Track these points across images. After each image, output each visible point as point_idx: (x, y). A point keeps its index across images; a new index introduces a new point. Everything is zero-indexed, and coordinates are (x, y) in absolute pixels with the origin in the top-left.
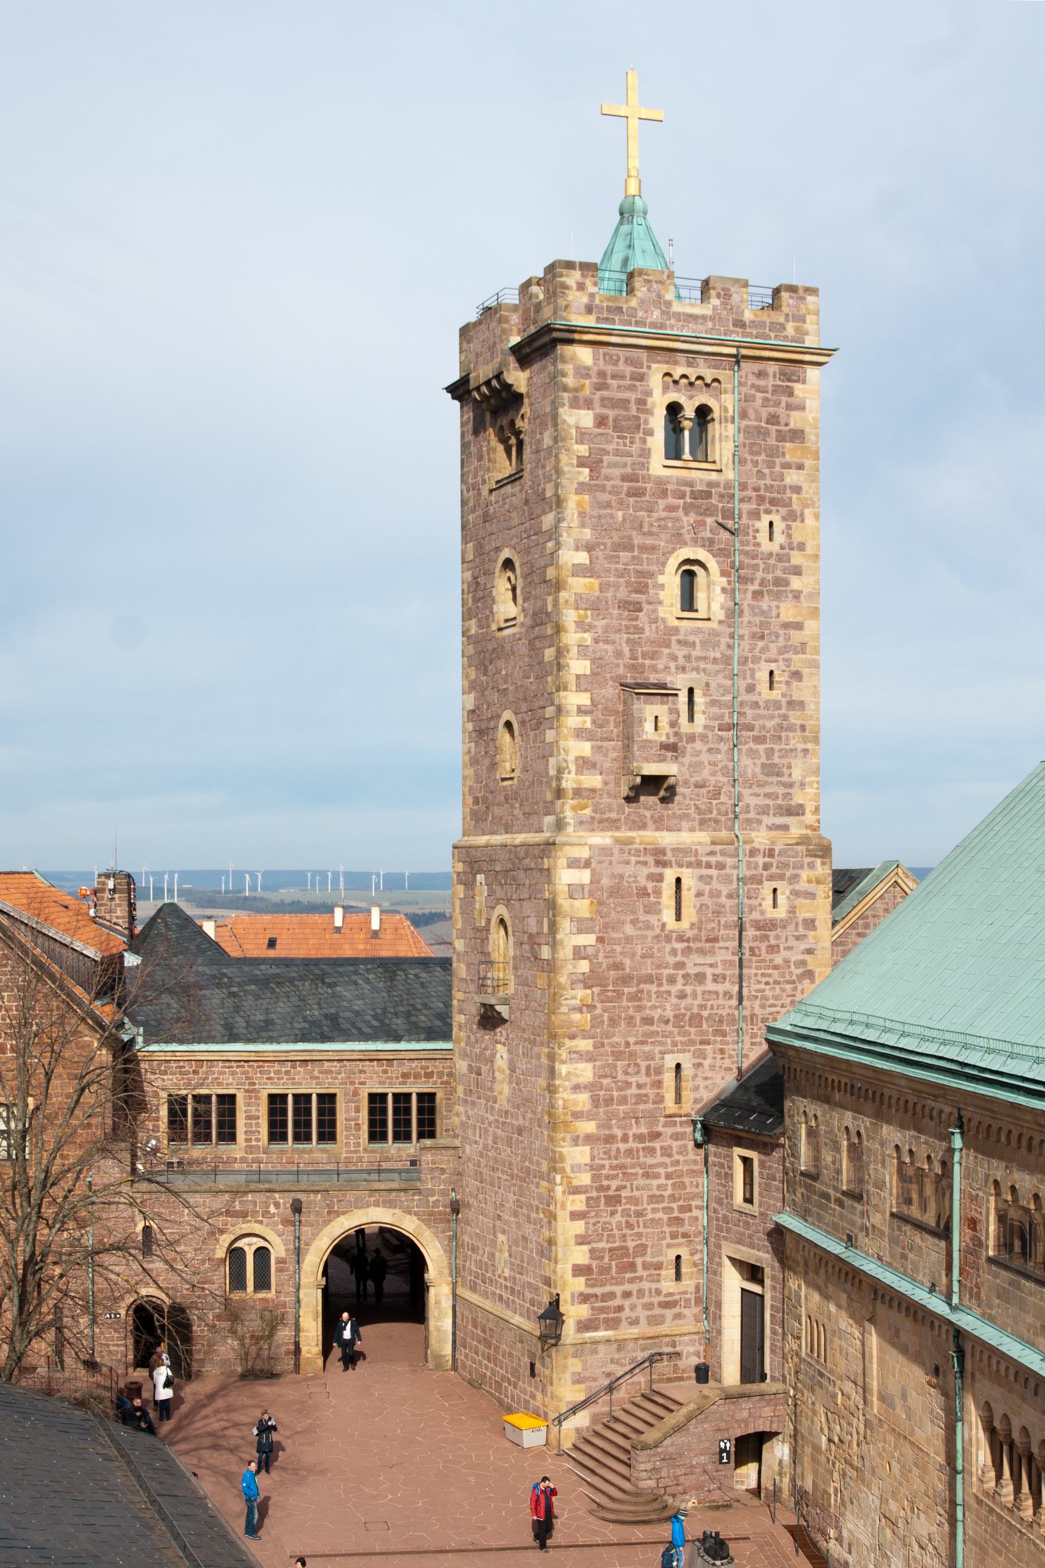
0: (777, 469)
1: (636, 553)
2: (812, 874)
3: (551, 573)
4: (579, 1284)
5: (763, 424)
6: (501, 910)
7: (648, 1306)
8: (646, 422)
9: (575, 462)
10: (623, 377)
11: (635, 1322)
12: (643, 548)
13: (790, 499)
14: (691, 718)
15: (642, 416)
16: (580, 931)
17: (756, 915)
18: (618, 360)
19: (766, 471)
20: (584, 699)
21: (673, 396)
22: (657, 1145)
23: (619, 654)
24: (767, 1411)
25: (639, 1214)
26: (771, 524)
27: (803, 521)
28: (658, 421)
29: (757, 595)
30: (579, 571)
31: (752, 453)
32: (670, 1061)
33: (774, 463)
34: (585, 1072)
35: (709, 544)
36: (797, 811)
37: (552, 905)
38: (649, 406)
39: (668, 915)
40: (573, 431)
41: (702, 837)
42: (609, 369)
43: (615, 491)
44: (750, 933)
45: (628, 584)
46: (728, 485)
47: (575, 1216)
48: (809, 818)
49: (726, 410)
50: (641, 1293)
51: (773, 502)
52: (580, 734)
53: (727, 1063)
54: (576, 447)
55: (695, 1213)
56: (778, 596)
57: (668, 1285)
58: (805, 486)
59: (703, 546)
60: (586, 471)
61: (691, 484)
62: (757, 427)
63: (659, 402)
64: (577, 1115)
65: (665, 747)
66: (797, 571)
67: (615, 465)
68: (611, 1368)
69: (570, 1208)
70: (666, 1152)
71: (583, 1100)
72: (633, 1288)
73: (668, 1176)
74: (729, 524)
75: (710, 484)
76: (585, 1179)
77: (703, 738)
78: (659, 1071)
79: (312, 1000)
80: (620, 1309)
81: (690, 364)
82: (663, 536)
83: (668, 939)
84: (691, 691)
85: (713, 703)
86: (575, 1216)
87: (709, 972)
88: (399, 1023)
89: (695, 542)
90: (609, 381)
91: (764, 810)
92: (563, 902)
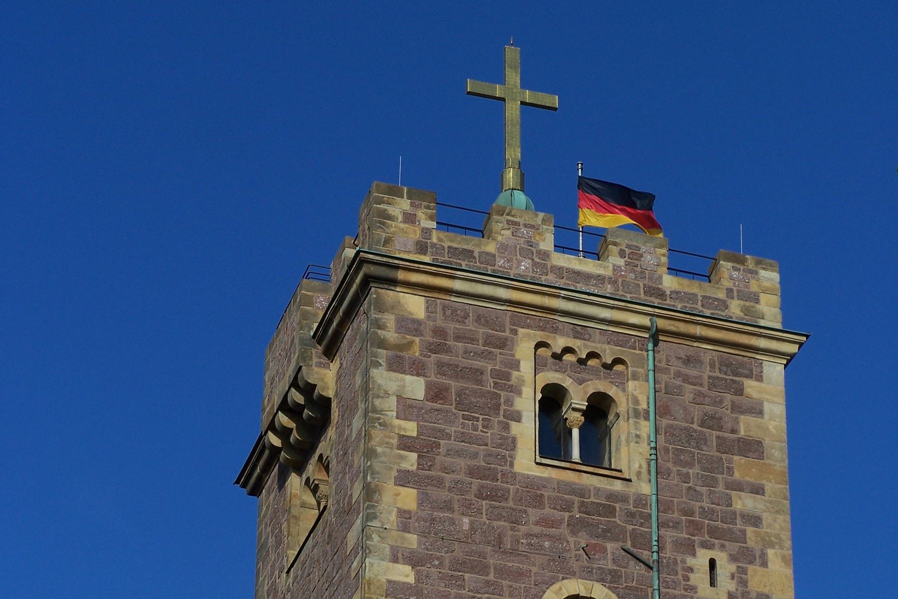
0: (721, 488)
1: (491, 577)
5: (695, 426)
8: (509, 402)
9: (395, 441)
10: (473, 340)
12: (501, 572)
13: (744, 532)
15: (503, 394)
18: (466, 316)
19: (704, 490)
21: (551, 377)
26: (712, 563)
27: (764, 564)
28: (527, 404)
31: (678, 462)
33: (715, 480)
38: (514, 380)
40: (392, 402)
42: (452, 327)
43: (458, 487)
46: (641, 501)
49: (636, 401)
51: (713, 532)
54: (397, 422)
58: (767, 518)
59: (601, 580)
60: (414, 456)
61: (582, 492)
62: (685, 429)
67: (459, 453)
74: (645, 554)
75: (613, 496)
81: (577, 336)
82: (539, 559)
89: (588, 574)
90: (451, 343)
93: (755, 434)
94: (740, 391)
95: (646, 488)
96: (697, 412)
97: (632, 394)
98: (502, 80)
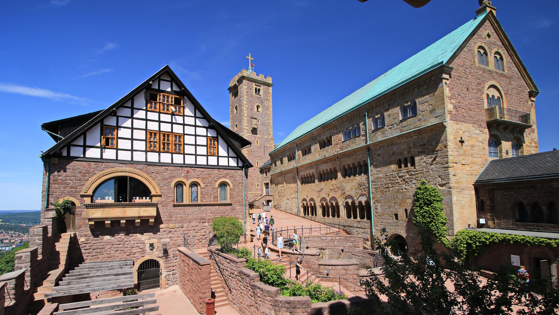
63: (255, 87)
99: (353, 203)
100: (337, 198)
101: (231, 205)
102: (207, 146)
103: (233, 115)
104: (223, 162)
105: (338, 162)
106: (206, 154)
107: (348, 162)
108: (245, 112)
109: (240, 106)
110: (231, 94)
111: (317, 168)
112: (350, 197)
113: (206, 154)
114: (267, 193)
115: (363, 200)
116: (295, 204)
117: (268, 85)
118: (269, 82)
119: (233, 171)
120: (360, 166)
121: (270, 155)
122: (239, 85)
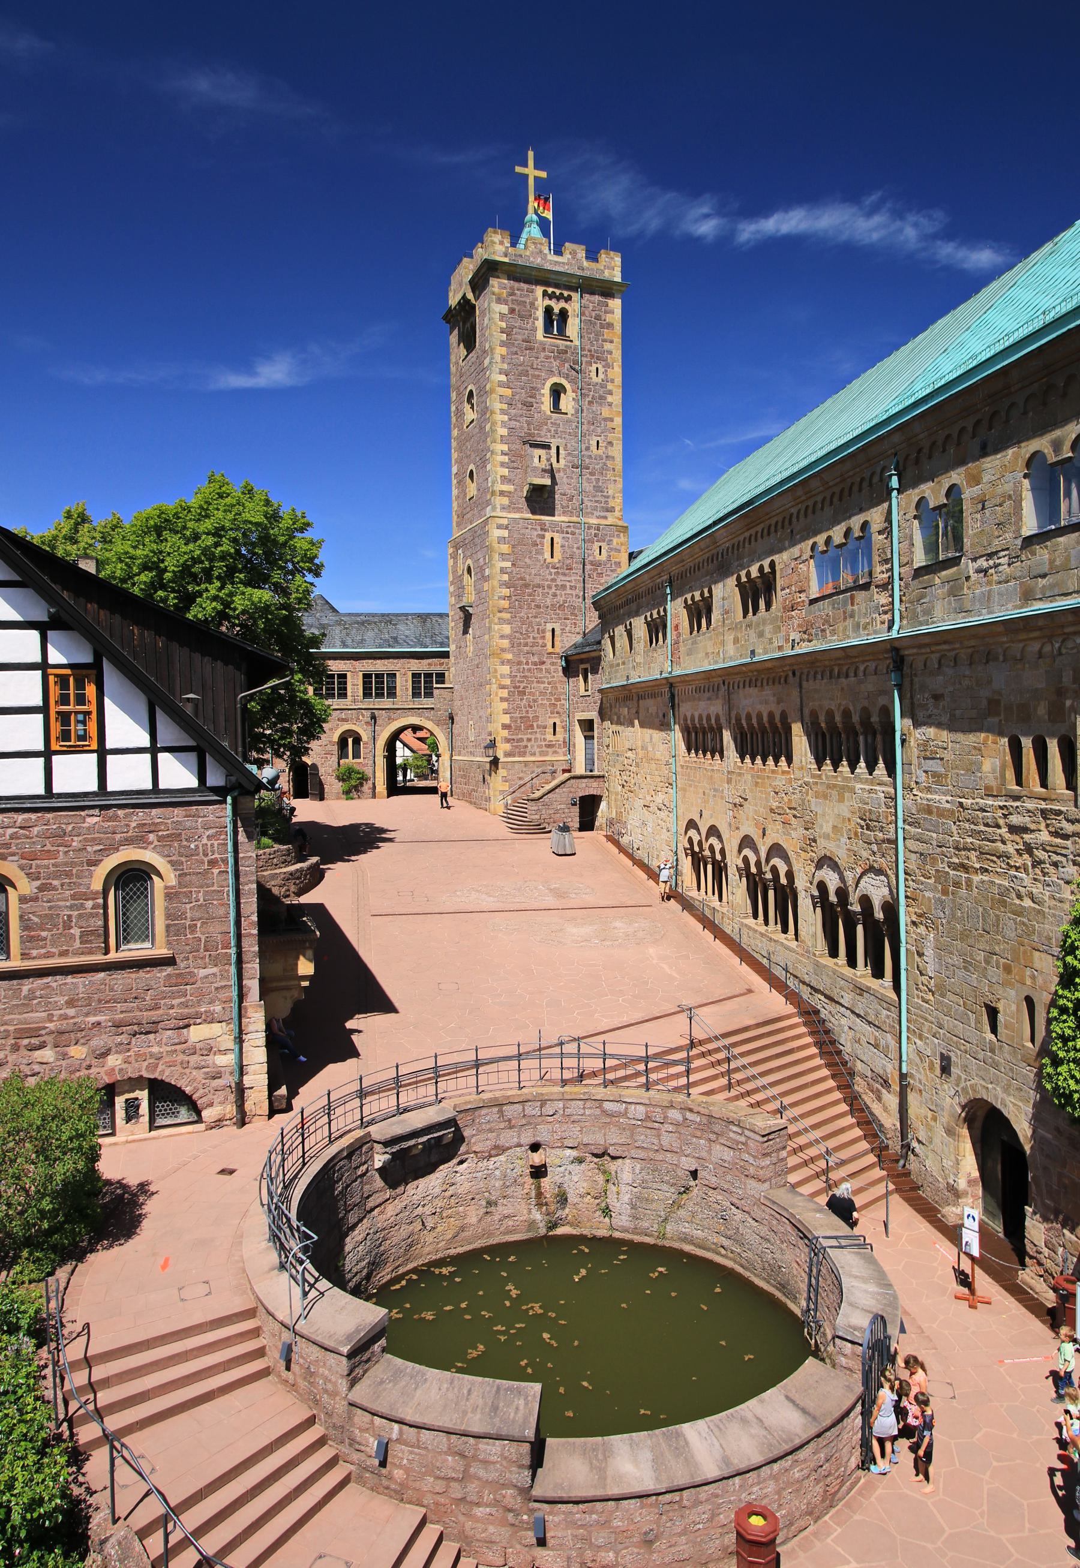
2: (619, 540)
3: (488, 388)
4: (505, 733)
6: (469, 562)
7: (540, 746)
11: (534, 754)
12: (534, 376)
14: (558, 461)
16: (503, 560)
17: (591, 558)
20: (505, 448)
22: (543, 667)
23: (521, 427)
24: (595, 784)
25: (535, 701)
28: (540, 314)
29: (590, 403)
30: (501, 384)
32: (549, 627)
34: (507, 629)
35: (567, 377)
36: (611, 510)
37: (489, 549)
39: (547, 555)
41: (566, 519)
42: (516, 285)
44: (588, 567)
45: (526, 393)
46: (576, 347)
47: (502, 699)
48: (617, 514)
50: (536, 739)
51: (598, 358)
52: (502, 464)
53: (578, 630)
55: (563, 702)
56: (601, 405)
57: (550, 737)
63: (541, 303)
64: (503, 650)
65: (544, 470)
66: (610, 393)
68: (521, 775)
69: (500, 695)
70: (548, 671)
71: (505, 643)
72: (533, 737)
73: (549, 683)
75: (566, 346)
76: (508, 682)
77: (564, 470)
78: (544, 631)
79: (385, 631)
80: (526, 747)
83: (548, 567)
84: (558, 448)
85: (569, 454)
86: (502, 699)
87: (568, 584)
88: (428, 641)
91: (595, 509)
92: (496, 545)
93: (612, 321)
94: (607, 306)
95: (577, 343)
96: (593, 314)
97: (573, 307)
98: (526, 165)
99: (842, 893)
100: (791, 854)
101: (170, 961)
102: (43, 709)
103: (460, 429)
104: (129, 774)
105: (795, 693)
106: (40, 746)
107: (831, 698)
108: (500, 418)
109: (483, 392)
110: (454, 338)
111: (729, 702)
112: (826, 861)
113: (40, 746)
114: (590, 762)
115: (877, 891)
116: (665, 835)
117: (606, 290)
118: (607, 275)
119: (176, 811)
120: (868, 728)
121: (596, 605)
122: (477, 298)
